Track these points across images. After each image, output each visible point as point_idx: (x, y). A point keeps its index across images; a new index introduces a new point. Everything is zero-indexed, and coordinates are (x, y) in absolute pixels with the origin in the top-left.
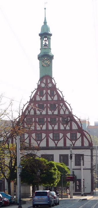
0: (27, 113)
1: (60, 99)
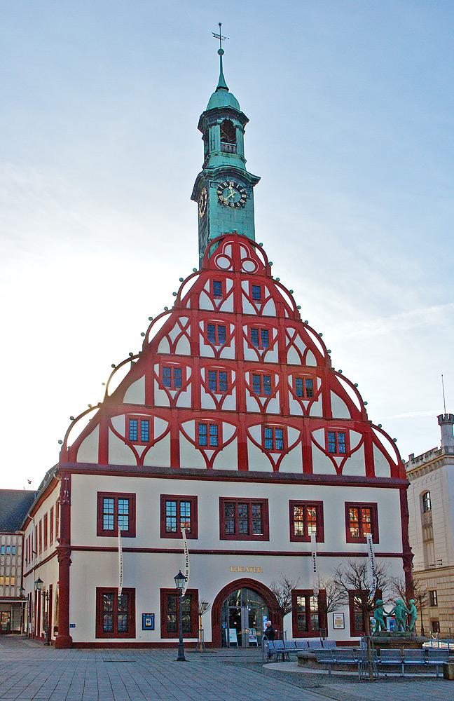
0: (164, 348)
1: (287, 316)
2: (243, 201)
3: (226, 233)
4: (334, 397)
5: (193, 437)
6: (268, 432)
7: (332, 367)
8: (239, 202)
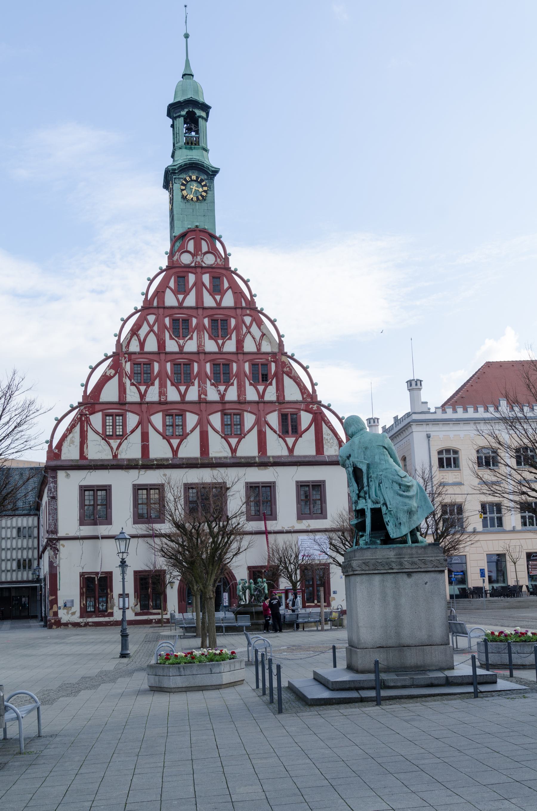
1: (244, 304)
2: (204, 194)
3: (189, 228)
4: (287, 381)
5: (160, 428)
6: (227, 419)
7: (285, 351)
8: (201, 195)
